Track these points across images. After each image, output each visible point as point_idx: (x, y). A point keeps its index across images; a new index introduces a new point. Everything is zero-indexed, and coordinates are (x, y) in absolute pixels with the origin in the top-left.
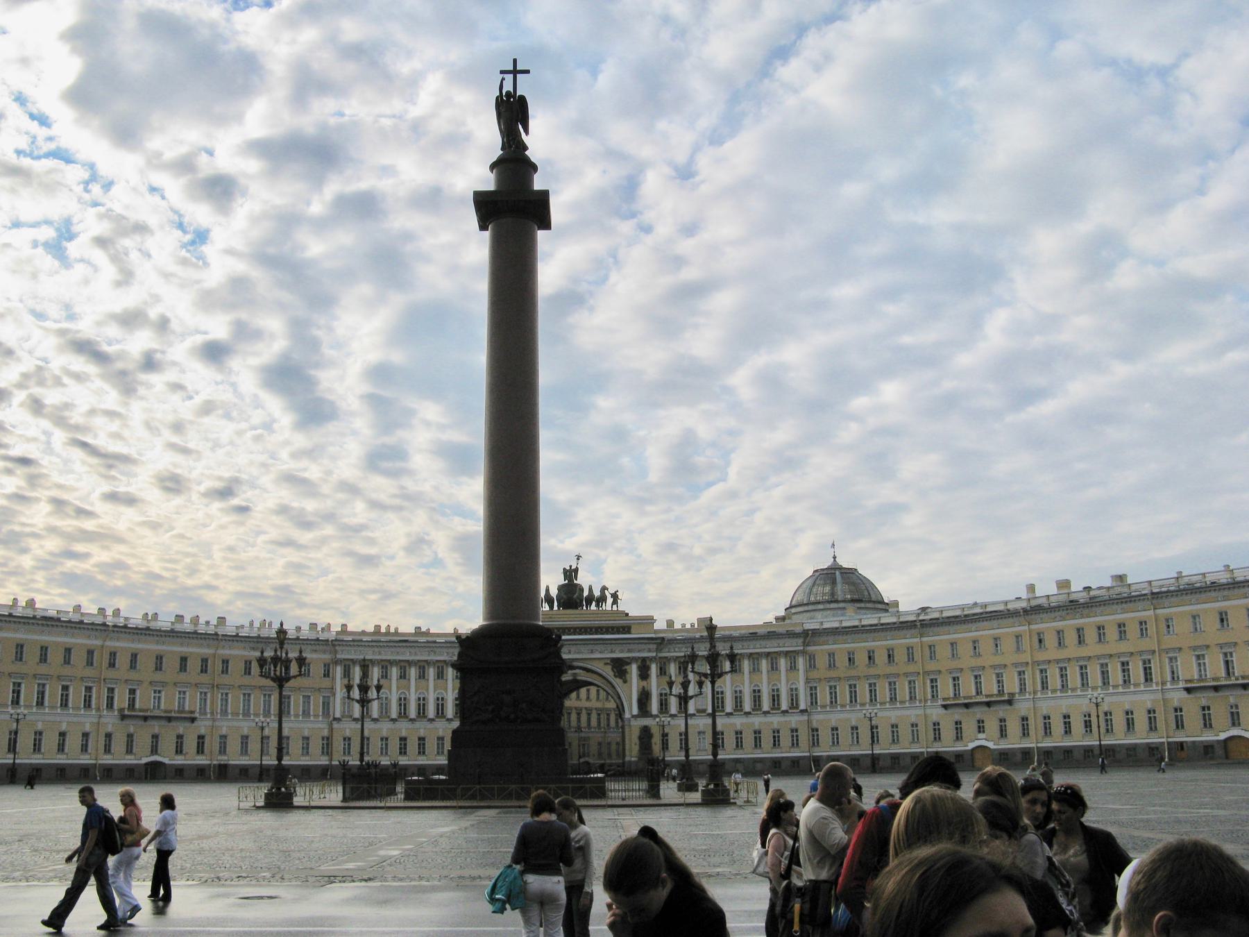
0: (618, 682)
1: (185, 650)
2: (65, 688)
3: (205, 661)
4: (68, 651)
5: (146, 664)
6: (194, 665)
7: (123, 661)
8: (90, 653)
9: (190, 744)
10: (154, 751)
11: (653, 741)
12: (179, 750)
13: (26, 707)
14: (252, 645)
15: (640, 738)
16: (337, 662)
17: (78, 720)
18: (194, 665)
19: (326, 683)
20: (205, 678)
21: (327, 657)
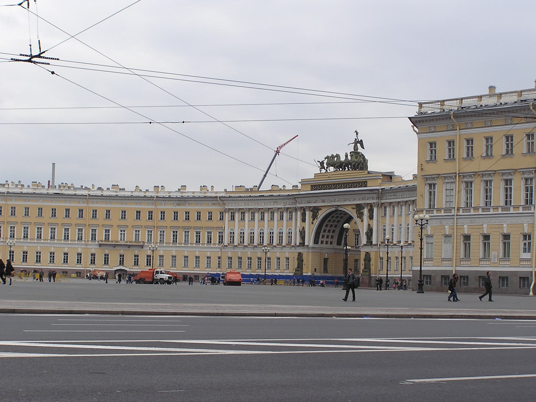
0: (358, 220)
1: (138, 207)
2: (67, 230)
3: (151, 213)
4: (68, 210)
5: (116, 216)
6: (145, 216)
7: (101, 215)
8: (81, 211)
9: (143, 260)
10: (122, 263)
11: (371, 263)
12: (136, 263)
13: (44, 240)
14: (177, 202)
15: (365, 260)
16: (226, 211)
17: (74, 248)
18: (145, 216)
19: (220, 224)
20: (150, 223)
21: (220, 208)
